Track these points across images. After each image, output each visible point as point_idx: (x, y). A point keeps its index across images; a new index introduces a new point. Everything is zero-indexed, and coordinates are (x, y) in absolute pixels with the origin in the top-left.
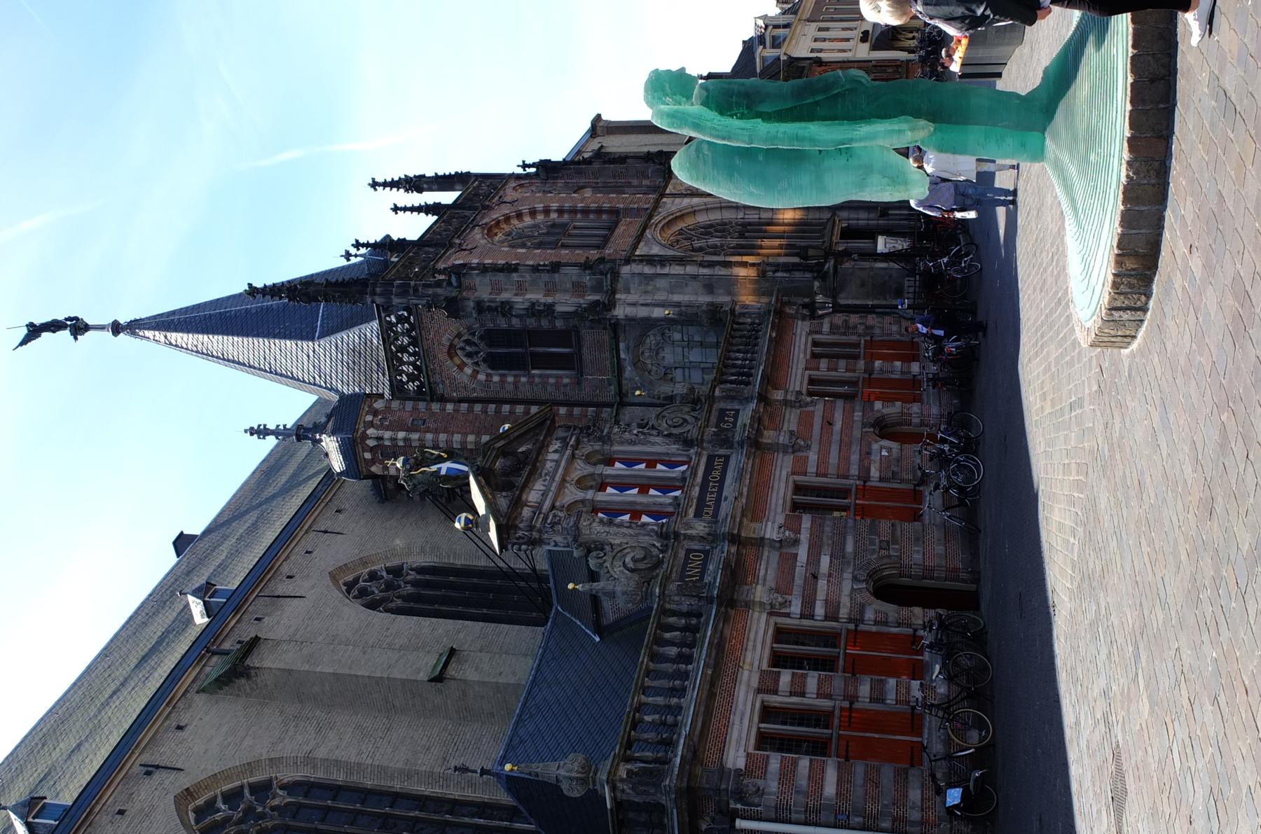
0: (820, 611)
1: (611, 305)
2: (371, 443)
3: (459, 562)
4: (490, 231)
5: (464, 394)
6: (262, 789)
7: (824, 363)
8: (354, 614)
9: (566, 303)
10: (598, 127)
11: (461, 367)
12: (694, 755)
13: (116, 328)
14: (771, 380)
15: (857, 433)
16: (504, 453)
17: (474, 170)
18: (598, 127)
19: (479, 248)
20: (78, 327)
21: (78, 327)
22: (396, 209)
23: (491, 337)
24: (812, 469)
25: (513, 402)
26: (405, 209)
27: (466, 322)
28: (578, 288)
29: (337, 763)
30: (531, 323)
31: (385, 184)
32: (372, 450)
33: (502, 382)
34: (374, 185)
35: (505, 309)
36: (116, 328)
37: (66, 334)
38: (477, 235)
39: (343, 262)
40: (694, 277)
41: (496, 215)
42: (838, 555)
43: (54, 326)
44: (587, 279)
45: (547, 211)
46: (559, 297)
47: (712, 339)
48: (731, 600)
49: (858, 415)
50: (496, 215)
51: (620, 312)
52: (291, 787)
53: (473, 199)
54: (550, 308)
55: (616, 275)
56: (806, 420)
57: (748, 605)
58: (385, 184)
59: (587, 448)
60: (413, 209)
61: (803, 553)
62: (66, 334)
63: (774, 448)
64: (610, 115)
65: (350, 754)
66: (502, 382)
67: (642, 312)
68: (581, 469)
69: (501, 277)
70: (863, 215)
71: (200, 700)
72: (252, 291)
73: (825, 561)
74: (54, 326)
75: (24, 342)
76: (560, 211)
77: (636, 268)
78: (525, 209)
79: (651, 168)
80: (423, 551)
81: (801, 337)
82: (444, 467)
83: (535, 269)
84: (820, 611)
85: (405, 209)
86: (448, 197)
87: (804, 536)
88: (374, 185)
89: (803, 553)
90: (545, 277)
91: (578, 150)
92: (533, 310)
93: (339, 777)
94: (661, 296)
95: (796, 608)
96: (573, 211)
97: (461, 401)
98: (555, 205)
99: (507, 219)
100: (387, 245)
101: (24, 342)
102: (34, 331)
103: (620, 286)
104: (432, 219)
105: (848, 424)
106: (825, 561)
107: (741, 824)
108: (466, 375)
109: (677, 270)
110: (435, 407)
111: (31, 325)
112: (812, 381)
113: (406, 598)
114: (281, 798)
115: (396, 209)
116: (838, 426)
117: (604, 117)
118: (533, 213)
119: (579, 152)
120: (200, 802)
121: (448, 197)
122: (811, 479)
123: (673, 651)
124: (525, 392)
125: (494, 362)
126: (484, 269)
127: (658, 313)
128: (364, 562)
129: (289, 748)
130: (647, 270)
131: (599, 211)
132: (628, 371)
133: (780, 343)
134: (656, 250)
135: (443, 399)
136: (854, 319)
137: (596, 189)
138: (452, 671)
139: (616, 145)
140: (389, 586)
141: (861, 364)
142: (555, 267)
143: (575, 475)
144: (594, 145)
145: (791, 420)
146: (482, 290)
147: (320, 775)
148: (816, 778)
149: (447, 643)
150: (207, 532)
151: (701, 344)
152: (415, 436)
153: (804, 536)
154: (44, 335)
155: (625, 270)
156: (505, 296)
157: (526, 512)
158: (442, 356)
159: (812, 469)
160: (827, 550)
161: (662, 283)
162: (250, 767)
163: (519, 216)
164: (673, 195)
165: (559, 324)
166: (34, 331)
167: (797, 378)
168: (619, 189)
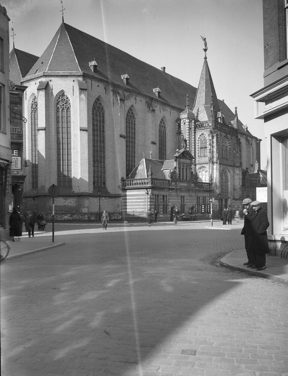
7: (202, 198)
13: (206, 58)
20: (205, 50)
31: (236, 110)
34: (236, 108)
36: (206, 58)
37: (204, 47)
43: (206, 45)
58: (236, 110)
62: (204, 47)
70: (230, 203)
74: (206, 45)
75: (202, 37)
88: (236, 108)
101: (202, 37)
111: (205, 39)
122: (185, 198)
145: (194, 194)
149: (156, 143)
150: (166, 73)
154: (203, 42)
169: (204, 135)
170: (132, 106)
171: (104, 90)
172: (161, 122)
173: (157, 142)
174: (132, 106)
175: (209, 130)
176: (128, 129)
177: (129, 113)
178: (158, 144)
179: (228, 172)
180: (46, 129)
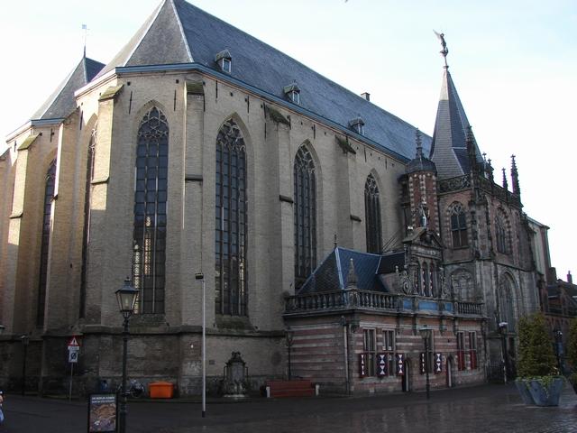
0: (398, 344)
1: (480, 260)
2: (420, 177)
3: (382, 213)
4: (500, 209)
5: (441, 207)
6: (312, 165)
8: (363, 180)
9: (479, 243)
10: (544, 229)
11: (451, 206)
12: (362, 313)
14: (461, 320)
15: (447, 350)
16: (432, 236)
17: (521, 195)
18: (544, 229)
19: (494, 206)
20: (445, 53)
21: (445, 53)
22: (504, 170)
23: (462, 215)
24: (436, 337)
25: (440, 227)
26: (504, 173)
27: (468, 208)
28: (483, 247)
29: (322, 189)
30: (470, 231)
31: (514, 161)
32: (418, 177)
33: (447, 221)
34: (513, 157)
35: (474, 222)
37: (442, 49)
38: (497, 204)
39: (482, 153)
40: (492, 288)
41: (506, 209)
42: (413, 348)
43: (444, 44)
44: (487, 250)
45: (509, 227)
46: (480, 241)
47: (470, 296)
48: (399, 317)
49: (453, 350)
50: (506, 209)
51: (477, 263)
52: (313, 175)
53: (512, 199)
54: (476, 238)
55: (490, 260)
56: (449, 333)
57: (398, 323)
58: (514, 161)
59: (434, 263)
60: (504, 176)
61: (413, 337)
62: (442, 49)
63: (441, 325)
64: (550, 233)
65: (325, 192)
66: (447, 221)
67: (478, 271)
68: (429, 262)
69: (485, 219)
71: (333, 137)
72: (469, 128)
73: (411, 344)
74: (444, 44)
75: (436, 33)
76: (509, 232)
77: (493, 267)
78: (509, 219)
79: (529, 263)
80: (385, 199)
81: (474, 328)
82: (425, 218)
83: (489, 231)
84: (398, 344)
85: (504, 173)
86: (510, 189)
87: (417, 337)
88: (513, 157)
89: (413, 337)
90: (486, 235)
91: (533, 222)
92: (475, 232)
93: (318, 190)
94: (484, 277)
95: (398, 337)
96: (510, 237)
97: (438, 207)
98: (511, 230)
99: (505, 213)
100: (490, 169)
101: (436, 33)
102: (442, 37)
103: (486, 262)
104: (501, 184)
105: (450, 347)
106: (411, 344)
107: (345, 328)
108: (447, 208)
109: (494, 282)
110: (435, 198)
112: (461, 334)
113: (369, 197)
114: (310, 172)
115: (504, 170)
116: (449, 344)
117: (549, 231)
118: (508, 222)
119: (532, 223)
120: (306, 147)
121: (510, 189)
123: (384, 302)
124: (444, 230)
125: (454, 217)
126: (487, 213)
127: (478, 276)
128: (378, 179)
129: (324, 171)
130: (493, 272)
131: (511, 247)
132: (456, 267)
133: (472, 321)
134: (499, 272)
135: (438, 200)
136: (483, 346)
137: (519, 243)
138: (355, 222)
139: (537, 239)
140: (372, 189)
141: (468, 350)
142: (490, 239)
143: (426, 261)
144: (536, 229)
145: (450, 329)
146: (479, 212)
147: (318, 184)
148: (358, 348)
151: (468, 292)
152: (425, 192)
153: (417, 337)
154: (440, 41)
155: (492, 264)
156: (478, 222)
157: (415, 248)
158: (454, 199)
159: (436, 337)
160: (416, 344)
161: (488, 277)
162: (317, 160)
163: (506, 217)
164: (519, 274)
165: (470, 241)
166: (442, 37)
167: (462, 328)
168: (520, 252)
169: (459, 205)
170: (308, 142)
171: (246, 103)
172: (369, 181)
173: (363, 217)
174: (308, 142)
175: (468, 192)
176: (299, 188)
177: (302, 156)
178: (363, 223)
179: (511, 282)
180: (111, 181)
